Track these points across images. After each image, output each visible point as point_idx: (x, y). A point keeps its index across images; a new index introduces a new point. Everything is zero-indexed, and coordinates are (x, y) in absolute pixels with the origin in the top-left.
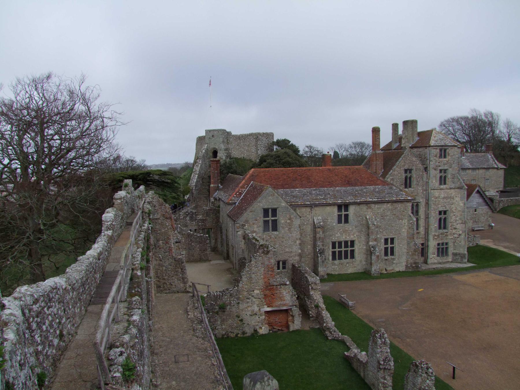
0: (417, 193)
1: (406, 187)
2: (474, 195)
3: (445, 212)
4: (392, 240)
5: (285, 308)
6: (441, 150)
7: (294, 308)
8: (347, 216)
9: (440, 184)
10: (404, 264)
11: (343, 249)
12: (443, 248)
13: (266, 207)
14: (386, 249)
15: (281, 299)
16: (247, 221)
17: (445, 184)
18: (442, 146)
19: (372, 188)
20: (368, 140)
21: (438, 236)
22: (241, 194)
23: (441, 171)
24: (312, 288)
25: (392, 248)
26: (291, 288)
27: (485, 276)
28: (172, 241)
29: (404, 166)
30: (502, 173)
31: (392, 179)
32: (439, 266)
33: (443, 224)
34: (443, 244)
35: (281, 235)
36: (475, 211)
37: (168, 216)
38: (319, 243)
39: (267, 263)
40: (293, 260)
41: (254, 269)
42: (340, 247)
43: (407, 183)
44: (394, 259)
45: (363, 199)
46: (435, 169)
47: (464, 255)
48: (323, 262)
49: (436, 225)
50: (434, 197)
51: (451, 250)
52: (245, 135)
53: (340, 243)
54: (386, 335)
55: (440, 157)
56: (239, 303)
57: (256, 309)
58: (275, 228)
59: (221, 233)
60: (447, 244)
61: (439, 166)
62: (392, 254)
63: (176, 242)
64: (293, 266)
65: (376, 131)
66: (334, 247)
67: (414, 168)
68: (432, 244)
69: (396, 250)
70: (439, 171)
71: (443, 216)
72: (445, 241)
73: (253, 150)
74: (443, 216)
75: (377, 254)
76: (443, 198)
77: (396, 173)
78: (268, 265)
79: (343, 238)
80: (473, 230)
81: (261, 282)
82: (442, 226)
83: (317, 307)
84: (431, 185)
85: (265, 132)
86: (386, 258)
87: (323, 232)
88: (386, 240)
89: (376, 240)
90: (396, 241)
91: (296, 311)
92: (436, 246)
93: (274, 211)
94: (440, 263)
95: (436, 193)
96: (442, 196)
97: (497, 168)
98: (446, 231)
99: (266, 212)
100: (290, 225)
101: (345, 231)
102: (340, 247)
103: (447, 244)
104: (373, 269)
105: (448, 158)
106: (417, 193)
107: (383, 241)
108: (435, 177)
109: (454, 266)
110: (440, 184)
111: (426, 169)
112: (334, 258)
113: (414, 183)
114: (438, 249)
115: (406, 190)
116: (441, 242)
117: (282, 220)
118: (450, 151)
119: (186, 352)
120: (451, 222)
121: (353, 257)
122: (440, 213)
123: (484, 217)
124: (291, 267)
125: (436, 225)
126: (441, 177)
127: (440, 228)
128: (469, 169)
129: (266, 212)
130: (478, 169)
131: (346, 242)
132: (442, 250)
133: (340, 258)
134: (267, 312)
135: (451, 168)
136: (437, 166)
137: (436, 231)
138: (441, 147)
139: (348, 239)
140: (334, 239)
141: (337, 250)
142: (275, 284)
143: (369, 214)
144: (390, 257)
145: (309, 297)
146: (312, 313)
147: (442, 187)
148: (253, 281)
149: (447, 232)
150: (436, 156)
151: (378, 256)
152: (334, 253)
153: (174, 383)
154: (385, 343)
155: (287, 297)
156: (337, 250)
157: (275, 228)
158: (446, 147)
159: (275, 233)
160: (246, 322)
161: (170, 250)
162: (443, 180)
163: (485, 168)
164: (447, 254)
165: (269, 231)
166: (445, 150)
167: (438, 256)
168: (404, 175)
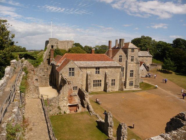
2: (142, 65)
3: (133, 71)
4: (114, 80)
5: (76, 104)
6: (132, 50)
7: (79, 104)
8: (99, 71)
9: (131, 61)
10: (118, 88)
11: (97, 83)
13: (70, 67)
14: (112, 83)
15: (74, 101)
16: (63, 72)
17: (133, 61)
19: (108, 62)
20: (107, 45)
21: (130, 79)
22: (61, 62)
23: (132, 57)
24: (86, 97)
25: (114, 83)
26: (78, 97)
27: (145, 93)
28: (34, 79)
30: (152, 58)
32: (130, 89)
33: (132, 75)
34: (131, 82)
35: (75, 78)
37: (33, 70)
38: (88, 81)
39: (70, 88)
40: (79, 87)
41: (65, 90)
42: (96, 82)
43: (120, 60)
44: (115, 87)
45: (105, 66)
47: (138, 86)
48: (90, 87)
49: (130, 75)
51: (134, 84)
53: (96, 81)
54: (111, 114)
56: (59, 102)
57: (65, 104)
58: (73, 75)
59: (53, 76)
60: (133, 82)
62: (114, 85)
63: (36, 80)
64: (79, 89)
65: (110, 42)
66: (94, 82)
68: (128, 82)
69: (115, 84)
71: (132, 72)
73: (67, 46)
74: (132, 72)
75: (109, 85)
78: (70, 88)
79: (97, 79)
80: (142, 77)
81: (67, 95)
83: (87, 104)
84: (128, 62)
86: (112, 86)
87: (90, 77)
88: (112, 80)
89: (108, 80)
90: (116, 81)
91: (80, 105)
93: (73, 69)
94: (130, 88)
95: (130, 64)
97: (150, 57)
99: (70, 69)
100: (79, 74)
101: (98, 77)
102: (96, 82)
103: (133, 82)
104: (107, 90)
107: (111, 80)
109: (134, 89)
110: (131, 61)
111: (127, 56)
112: (94, 86)
114: (130, 83)
117: (76, 72)
118: (135, 50)
119: (38, 121)
121: (100, 86)
122: (131, 71)
124: (78, 89)
127: (130, 76)
128: (141, 56)
129: (70, 69)
130: (144, 57)
131: (98, 80)
132: (131, 84)
133: (96, 86)
134: (69, 106)
139: (100, 79)
140: (94, 80)
141: (95, 83)
142: (72, 95)
143: (107, 71)
144: (113, 86)
145: (85, 100)
146: (86, 106)
147: (132, 62)
148: (65, 94)
151: (109, 86)
152: (94, 84)
153: (32, 133)
154: (111, 117)
155: (77, 100)
156: (95, 83)
157: (73, 75)
159: (73, 77)
160: (61, 109)
161: (33, 82)
162: (132, 60)
163: (146, 57)
164: (133, 85)
165: (71, 76)
166: (133, 50)
167: (130, 86)
168: (119, 58)
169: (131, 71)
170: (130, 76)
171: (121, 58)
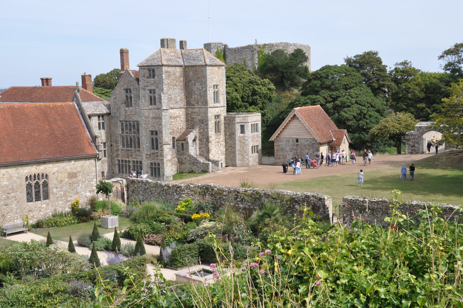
0: (136, 112)
1: (128, 106)
12: (155, 168)
18: (149, 66)
21: (150, 155)
29: (124, 85)
31: (115, 98)
36: (297, 141)
43: (128, 102)
46: (144, 89)
50: (144, 116)
52: (242, 48)
55: (150, 75)
60: (159, 165)
61: (147, 86)
67: (131, 88)
70: (148, 92)
71: (154, 137)
72: (157, 162)
76: (152, 118)
77: (117, 92)
82: (155, 146)
85: (267, 43)
92: (149, 165)
96: (151, 116)
98: (157, 151)
105: (156, 77)
106: (136, 112)
108: (144, 97)
110: (151, 104)
113: (133, 102)
114: (152, 168)
115: (127, 109)
116: (152, 162)
120: (160, 143)
122: (152, 132)
123: (309, 149)
125: (147, 145)
126: (151, 98)
127: (153, 148)
135: (157, 88)
136: (145, 86)
137: (147, 150)
138: (148, 67)
147: (151, 107)
149: (157, 153)
150: (144, 76)
158: (152, 67)
166: (154, 71)
169: (152, 132)
170: (153, 148)
171: (131, 97)
